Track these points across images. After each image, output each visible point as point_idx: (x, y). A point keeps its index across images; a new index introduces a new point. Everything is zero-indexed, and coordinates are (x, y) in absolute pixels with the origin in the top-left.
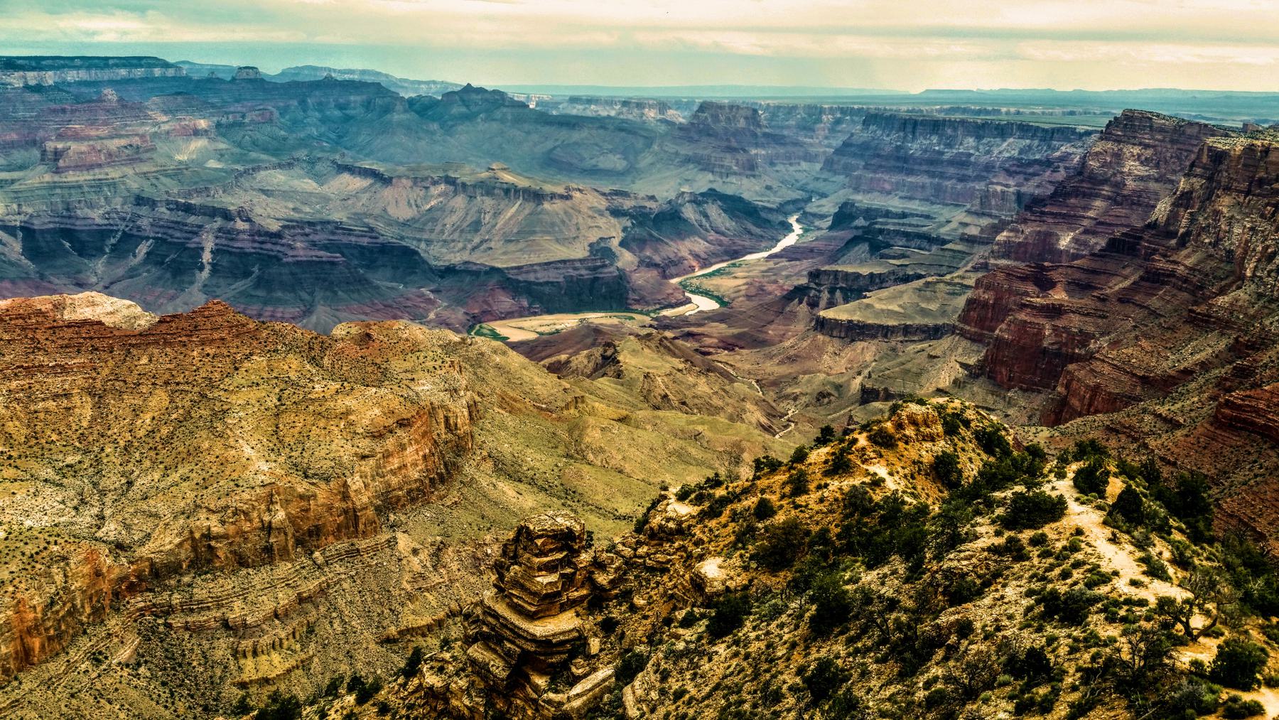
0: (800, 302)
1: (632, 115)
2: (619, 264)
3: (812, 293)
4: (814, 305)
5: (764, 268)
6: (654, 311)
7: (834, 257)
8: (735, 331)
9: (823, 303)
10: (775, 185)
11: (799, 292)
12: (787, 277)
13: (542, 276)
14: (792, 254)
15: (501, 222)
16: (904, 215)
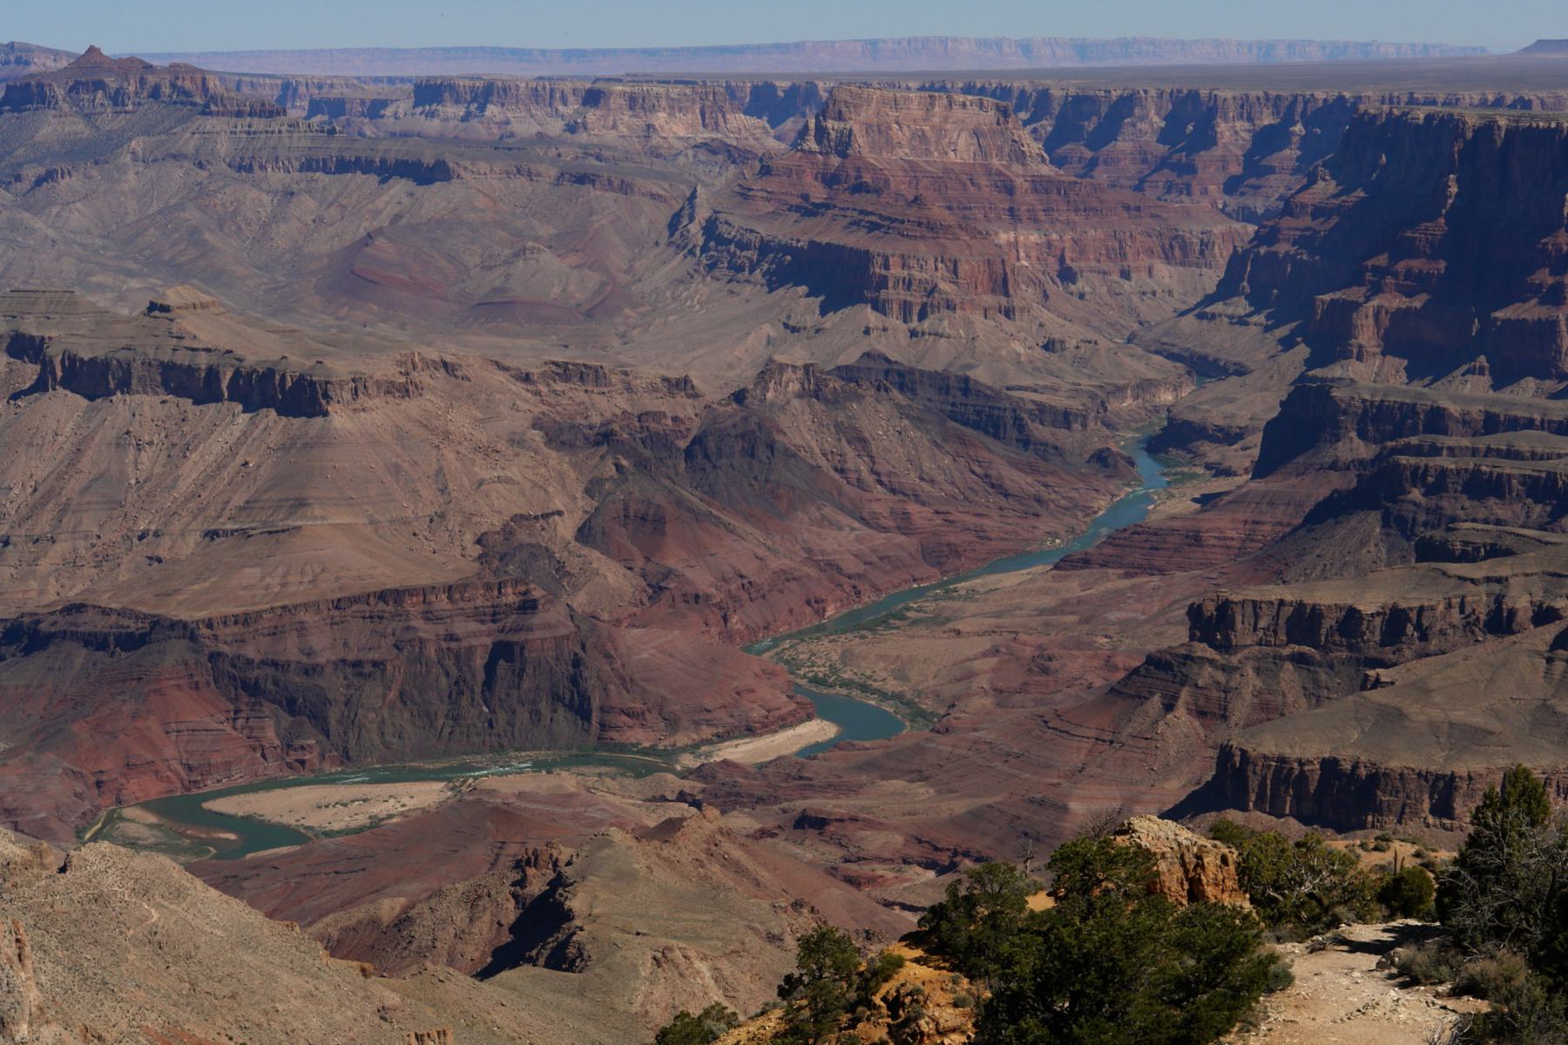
0: (1169, 707)
1: (611, 129)
2: (580, 601)
3: (1205, 675)
4: (1210, 712)
5: (1048, 601)
6: (693, 748)
7: (1273, 559)
8: (960, 806)
9: (1241, 709)
10: (1073, 334)
11: (1162, 671)
12: (1124, 625)
13: (324, 645)
14: (1139, 549)
15: (191, 470)
16: (1492, 424)
